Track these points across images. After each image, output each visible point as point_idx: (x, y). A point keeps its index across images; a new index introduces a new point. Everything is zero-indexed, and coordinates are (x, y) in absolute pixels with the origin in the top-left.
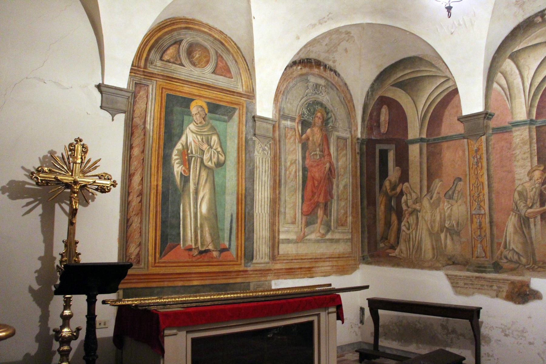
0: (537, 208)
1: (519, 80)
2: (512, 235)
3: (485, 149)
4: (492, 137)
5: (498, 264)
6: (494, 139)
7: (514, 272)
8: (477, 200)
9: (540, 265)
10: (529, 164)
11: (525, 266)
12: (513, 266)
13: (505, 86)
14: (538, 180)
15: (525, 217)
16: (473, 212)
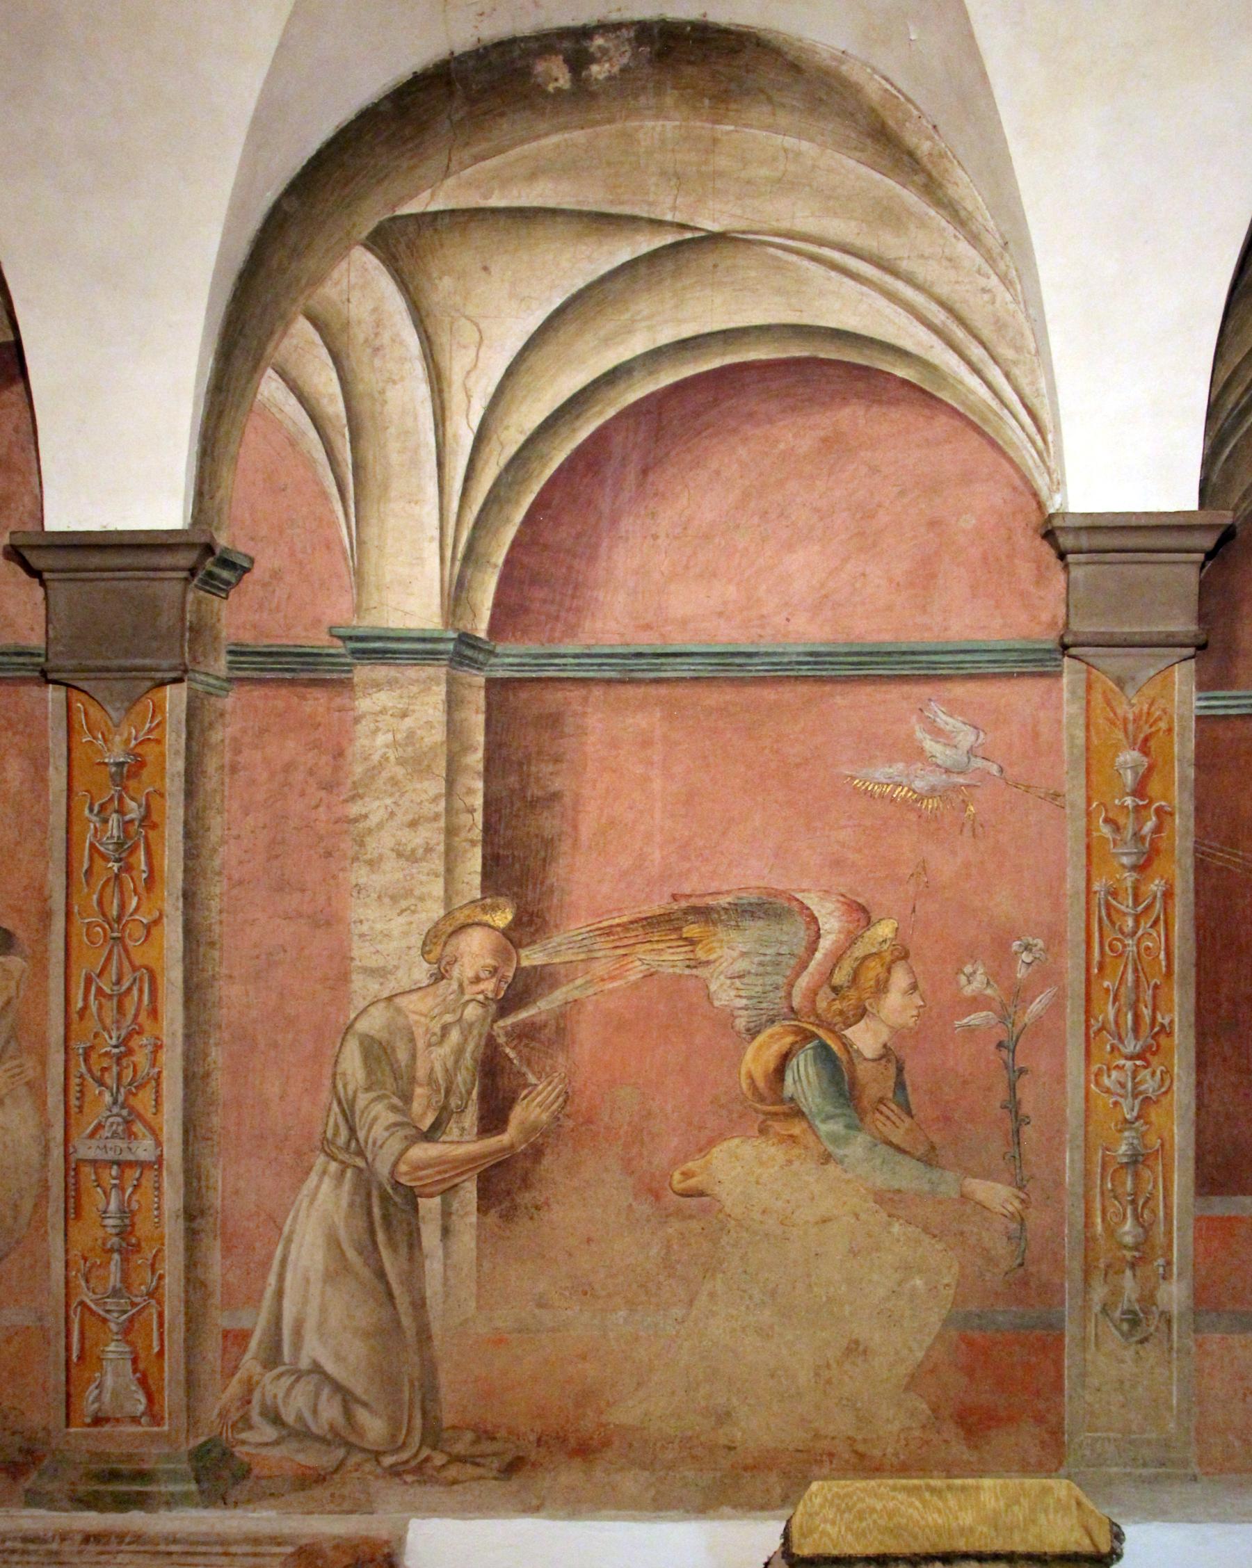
0: (463, 1142)
1: (424, 390)
2: (315, 1289)
3: (176, 765)
4: (229, 702)
5: (227, 1455)
6: (237, 712)
7: (318, 1492)
8: (110, 1079)
9: (460, 1448)
10: (438, 888)
11: (377, 1455)
12: (312, 1458)
13: (335, 408)
14: (477, 980)
15: (397, 1185)
16: (86, 1150)
